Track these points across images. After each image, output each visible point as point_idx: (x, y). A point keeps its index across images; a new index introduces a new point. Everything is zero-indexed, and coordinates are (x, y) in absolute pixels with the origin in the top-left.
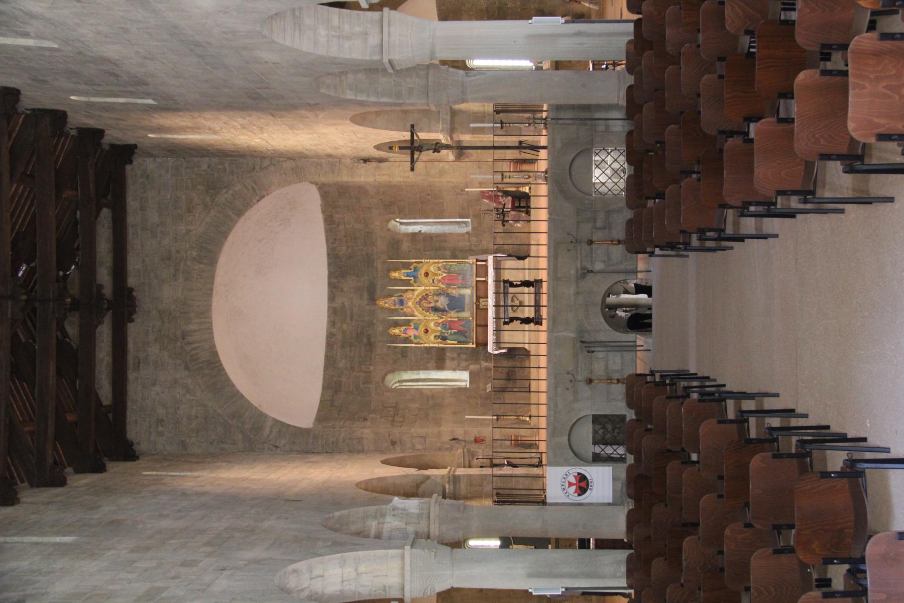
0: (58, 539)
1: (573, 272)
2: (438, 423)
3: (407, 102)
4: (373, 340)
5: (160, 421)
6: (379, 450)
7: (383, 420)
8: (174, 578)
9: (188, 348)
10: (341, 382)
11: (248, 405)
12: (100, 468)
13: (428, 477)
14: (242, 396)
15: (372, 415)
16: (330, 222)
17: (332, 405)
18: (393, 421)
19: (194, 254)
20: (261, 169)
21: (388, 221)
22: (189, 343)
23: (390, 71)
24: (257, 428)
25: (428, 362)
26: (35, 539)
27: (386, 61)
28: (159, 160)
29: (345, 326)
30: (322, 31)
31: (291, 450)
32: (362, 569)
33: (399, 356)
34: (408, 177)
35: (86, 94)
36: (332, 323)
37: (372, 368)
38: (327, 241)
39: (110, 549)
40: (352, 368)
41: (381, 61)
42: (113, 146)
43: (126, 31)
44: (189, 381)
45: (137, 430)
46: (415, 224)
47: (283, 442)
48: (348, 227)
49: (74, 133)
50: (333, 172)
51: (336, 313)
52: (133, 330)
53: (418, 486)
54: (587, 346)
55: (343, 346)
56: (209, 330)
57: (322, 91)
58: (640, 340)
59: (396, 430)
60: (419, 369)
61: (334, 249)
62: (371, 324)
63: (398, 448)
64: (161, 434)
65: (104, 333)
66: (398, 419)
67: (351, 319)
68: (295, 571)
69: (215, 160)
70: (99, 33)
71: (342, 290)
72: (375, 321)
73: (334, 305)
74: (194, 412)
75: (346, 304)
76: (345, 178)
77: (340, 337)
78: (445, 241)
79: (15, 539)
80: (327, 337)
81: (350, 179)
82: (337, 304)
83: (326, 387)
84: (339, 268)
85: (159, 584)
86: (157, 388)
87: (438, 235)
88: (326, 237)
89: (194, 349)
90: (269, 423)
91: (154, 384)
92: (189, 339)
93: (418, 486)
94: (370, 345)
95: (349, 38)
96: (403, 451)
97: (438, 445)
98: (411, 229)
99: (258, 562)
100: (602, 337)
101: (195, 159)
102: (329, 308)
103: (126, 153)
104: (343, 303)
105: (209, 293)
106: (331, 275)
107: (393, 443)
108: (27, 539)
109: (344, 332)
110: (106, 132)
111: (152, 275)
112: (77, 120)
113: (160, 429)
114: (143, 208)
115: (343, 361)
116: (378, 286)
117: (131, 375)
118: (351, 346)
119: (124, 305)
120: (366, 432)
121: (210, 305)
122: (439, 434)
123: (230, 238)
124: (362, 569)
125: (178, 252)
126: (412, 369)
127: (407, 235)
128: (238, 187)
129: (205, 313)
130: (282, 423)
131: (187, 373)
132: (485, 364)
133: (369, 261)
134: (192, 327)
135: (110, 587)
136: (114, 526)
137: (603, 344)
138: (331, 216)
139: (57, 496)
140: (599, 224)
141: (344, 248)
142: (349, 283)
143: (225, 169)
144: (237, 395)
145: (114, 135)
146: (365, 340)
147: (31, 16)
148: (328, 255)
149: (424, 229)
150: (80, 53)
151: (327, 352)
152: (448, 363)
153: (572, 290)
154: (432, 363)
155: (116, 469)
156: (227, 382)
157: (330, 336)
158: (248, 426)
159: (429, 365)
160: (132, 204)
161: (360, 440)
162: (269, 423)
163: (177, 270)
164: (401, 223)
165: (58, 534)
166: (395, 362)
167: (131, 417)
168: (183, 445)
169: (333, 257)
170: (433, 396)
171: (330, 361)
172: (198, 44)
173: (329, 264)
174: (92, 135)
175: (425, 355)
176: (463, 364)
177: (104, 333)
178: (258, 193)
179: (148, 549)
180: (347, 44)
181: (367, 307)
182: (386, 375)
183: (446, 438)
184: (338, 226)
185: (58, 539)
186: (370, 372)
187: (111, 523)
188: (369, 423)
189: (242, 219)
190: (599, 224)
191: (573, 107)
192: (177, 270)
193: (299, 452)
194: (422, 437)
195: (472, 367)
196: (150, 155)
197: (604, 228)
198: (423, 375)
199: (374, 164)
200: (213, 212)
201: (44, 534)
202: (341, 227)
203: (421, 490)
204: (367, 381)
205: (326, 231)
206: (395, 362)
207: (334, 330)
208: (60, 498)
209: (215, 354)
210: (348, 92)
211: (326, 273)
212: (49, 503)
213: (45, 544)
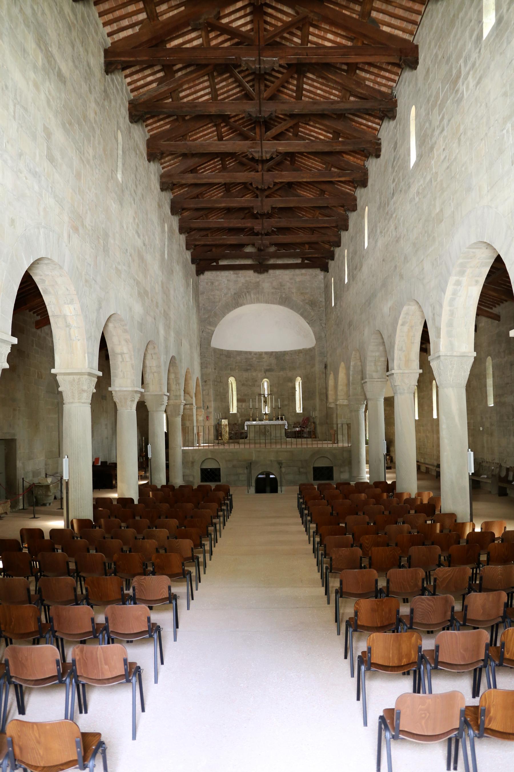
0: (166, 252)
1: (280, 459)
3: (351, 387)
5: (212, 283)
6: (202, 375)
8: (152, 300)
9: (244, 294)
10: (230, 358)
11: (219, 320)
12: (193, 262)
13: (192, 398)
14: (224, 317)
16: (300, 352)
17: (221, 355)
18: (215, 381)
19: (284, 296)
20: (321, 323)
22: (245, 294)
23: (362, 382)
24: (210, 324)
26: (166, 243)
27: (366, 380)
28: (323, 281)
29: (254, 359)
30: (377, 354)
31: (201, 338)
32: (155, 374)
35: (348, 256)
36: (256, 353)
37: (237, 371)
38: (291, 351)
39: (162, 273)
40: (236, 363)
41: (366, 378)
42: (327, 263)
43: (373, 276)
44: (230, 295)
45: (208, 275)
47: (205, 335)
49: (332, 249)
51: (260, 355)
52: (251, 273)
53: (188, 394)
54: (250, 465)
55: (246, 358)
56: (251, 303)
57: (354, 352)
58: (253, 489)
59: (211, 383)
61: (288, 354)
62: (256, 370)
63: (203, 383)
64: (207, 284)
65: (249, 262)
66: (216, 383)
68: (154, 347)
69: (324, 304)
70: (371, 265)
73: (264, 354)
74: (217, 297)
76: (317, 359)
77: (250, 357)
79: (167, 236)
82: (264, 355)
83: (228, 351)
84: (279, 357)
85: (150, 295)
86: (226, 282)
89: (243, 297)
90: (212, 328)
91: (228, 280)
92: (247, 294)
93: (188, 394)
94: (247, 370)
95: (375, 365)
96: (202, 386)
99: (158, 332)
100: (253, 472)
101: (324, 296)
102: (262, 352)
103: (325, 269)
104: (264, 358)
105: (267, 302)
106: (276, 352)
107: (205, 382)
108: (166, 240)
109: (252, 359)
110: (333, 261)
111: (274, 279)
112: (337, 251)
113: (209, 284)
114: (302, 274)
117: (232, 272)
119: (261, 268)
120: (210, 370)
121: (262, 303)
122: (210, 401)
123: (291, 311)
124: (155, 374)
125: (284, 289)
128: (313, 313)
129: (258, 301)
130: (213, 334)
131: (233, 294)
132: (240, 420)
134: (252, 296)
135: (149, 277)
136: (171, 272)
137: (250, 473)
138: (302, 352)
139: (182, 247)
140: (302, 470)
142: (273, 361)
143: (320, 308)
144: (224, 314)
145: (332, 264)
146: (249, 368)
147: (376, 242)
148: (285, 351)
149: (297, 393)
150: (363, 257)
151: (243, 352)
152: (241, 404)
153: (272, 459)
155: (193, 267)
156: (230, 310)
157: (250, 353)
158: (211, 320)
160: (303, 271)
161: (206, 367)
162: (212, 328)
163: (276, 289)
165: (168, 251)
166: (240, 381)
167: (214, 273)
168: (203, 293)
169: (284, 354)
171: (240, 353)
172: (369, 304)
173: (281, 352)
174: (332, 256)
176: (240, 411)
177: (249, 262)
178: (311, 323)
179: (163, 287)
180: (373, 364)
185: (166, 252)
187: (172, 271)
188: (214, 371)
189: (299, 316)
190: (302, 470)
191: (350, 457)
192: (276, 289)
193: (201, 341)
195: (239, 414)
196: (325, 277)
197: (299, 472)
198: (235, 393)
200: (301, 303)
201: (168, 247)
202: (297, 357)
203: (186, 395)
204: (231, 369)
205: (295, 350)
206: (240, 381)
207: (253, 354)
208: (181, 248)
209: (241, 305)
210: (354, 363)
212: (180, 245)
213: (164, 248)
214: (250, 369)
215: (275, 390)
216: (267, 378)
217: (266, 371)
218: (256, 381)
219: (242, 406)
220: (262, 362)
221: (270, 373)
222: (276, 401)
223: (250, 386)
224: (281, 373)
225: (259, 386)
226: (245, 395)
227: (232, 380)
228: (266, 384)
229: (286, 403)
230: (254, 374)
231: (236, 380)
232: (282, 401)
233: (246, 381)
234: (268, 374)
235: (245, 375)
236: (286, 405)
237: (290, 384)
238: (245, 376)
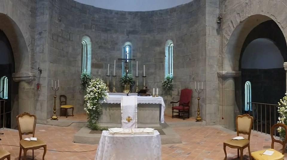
2: (54, 61)
7: (59, 30)
15: (64, 25)
18: (58, 36)
21: (172, 40)
25: (96, 59)
29: (115, 19)
33: (100, 45)
34: (208, 46)
36: (117, 13)
37: (94, 30)
38: (161, 10)
40: (93, 20)
46: (169, 54)
48: (169, 20)
50: (211, 3)
51: (122, 15)
60: (92, 54)
62: (116, 31)
66: (60, 39)
67: (119, 22)
72: (118, 33)
75: (127, 20)
78: (160, 69)
80: (110, 10)
81: (207, 12)
87: (163, 66)
88: (164, 10)
94: (106, 31)
97: (38, 61)
98: (167, 52)
102: (126, 12)
104: (127, 19)
109: (113, 18)
115: (98, 17)
116: (136, 36)
118: (105, 21)
126: (92, 51)
127: (164, 49)
133: (150, 31)
138: (175, 11)
141: (157, 19)
146: (108, 28)
148: (153, 11)
149: (167, 58)
152: (96, 70)
154: (95, 61)
157: (111, 12)
159: (94, 60)
164: (169, 47)
166: (97, 42)
169: (152, 14)
170: (76, 60)
175: (100, 58)
181: (125, 30)
182: (89, 37)
183: (42, 68)
184: (169, 15)
186: (91, 29)
188: (57, 22)
194: (43, 50)
198: (89, 56)
199: (216, 26)
202: (169, 17)
204: (86, 27)
205: (167, 10)
206: (97, 42)
207: (113, 14)
211: (143, 11)
214: (109, 30)
215: (139, 55)
216: (129, 41)
217: (129, 33)
218: (116, 44)
219: (98, 72)
220: (125, 22)
221: (133, 36)
222: (141, 67)
224: (148, 36)
225: (120, 50)
226: (102, 60)
227: (86, 41)
228: (127, 49)
229: (152, 70)
230: (114, 36)
231: (91, 41)
232: (148, 68)
234: (131, 36)
235: (104, 36)
236: (152, 74)
237: (158, 49)
238: (103, 38)
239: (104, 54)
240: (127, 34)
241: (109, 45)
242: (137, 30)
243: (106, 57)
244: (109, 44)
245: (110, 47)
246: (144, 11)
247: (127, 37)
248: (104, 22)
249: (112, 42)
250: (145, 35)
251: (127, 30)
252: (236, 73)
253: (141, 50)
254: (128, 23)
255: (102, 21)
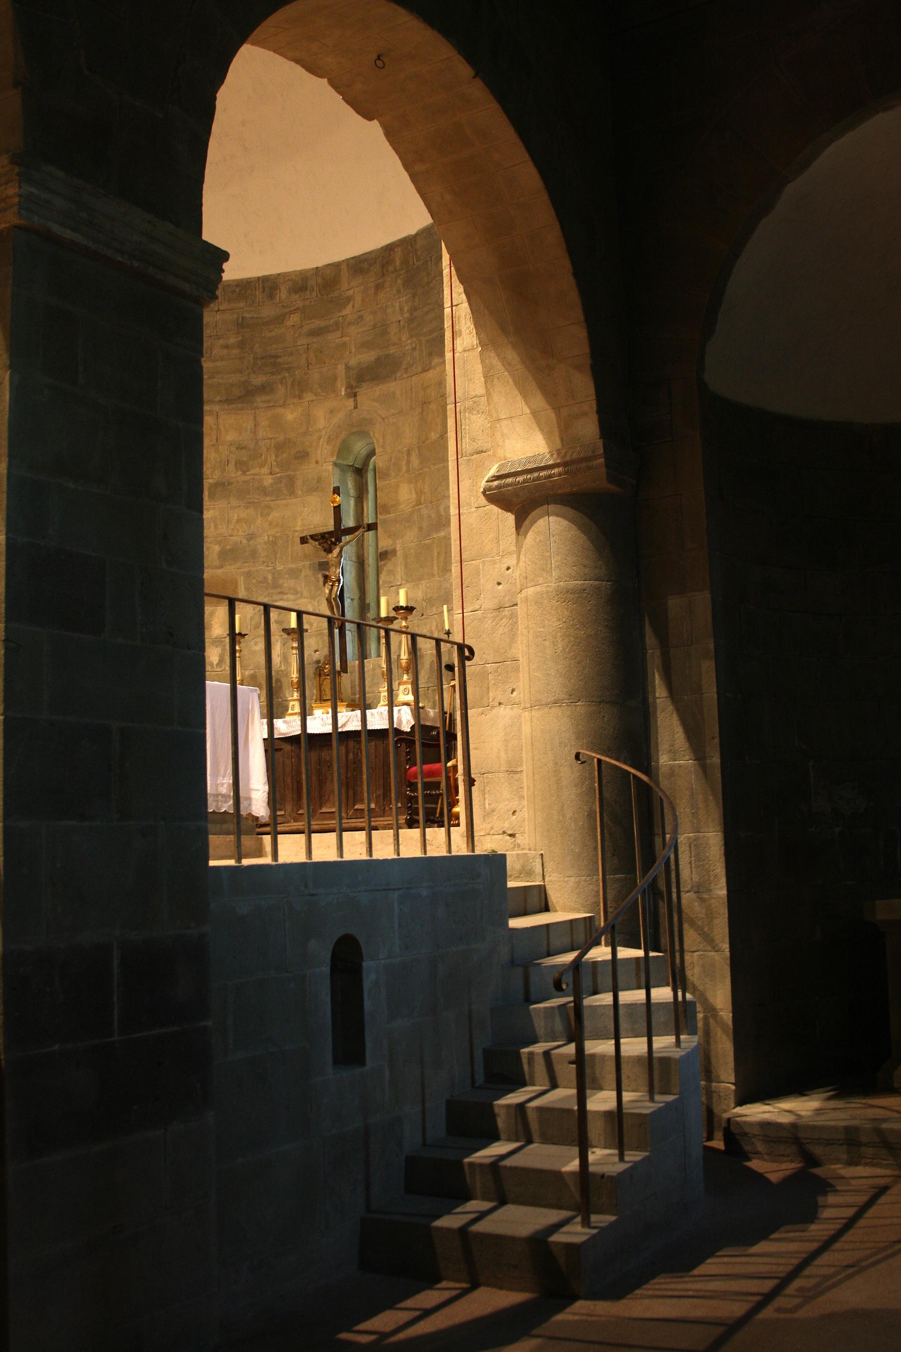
4: (259, 400)
29: (295, 319)
36: (300, 283)
55: (241, 324)
62: (300, 388)
67: (317, 332)
71: (378, 287)
72: (309, 396)
73: (345, 273)
75: (347, 311)
77: (268, 311)
80: (265, 280)
102: (337, 266)
104: (349, 299)
109: (280, 320)
116: (392, 386)
118: (241, 345)
146: (258, 380)
181: (341, 368)
207: (283, 293)
214: (263, 389)
218: (303, 456)
223: (264, 491)
230: (290, 415)
233: (242, 466)
234: (369, 395)
238: (230, 437)
239: (239, 520)
240: (349, 387)
241: (265, 470)
242: (392, 351)
243: (251, 537)
244: (262, 466)
245: (268, 481)
246: (413, 231)
247: (350, 403)
248: (235, 352)
249: (279, 447)
250: (425, 370)
251: (347, 368)
252: (565, 464)
253: (415, 461)
254: (350, 324)
255: (227, 347)
